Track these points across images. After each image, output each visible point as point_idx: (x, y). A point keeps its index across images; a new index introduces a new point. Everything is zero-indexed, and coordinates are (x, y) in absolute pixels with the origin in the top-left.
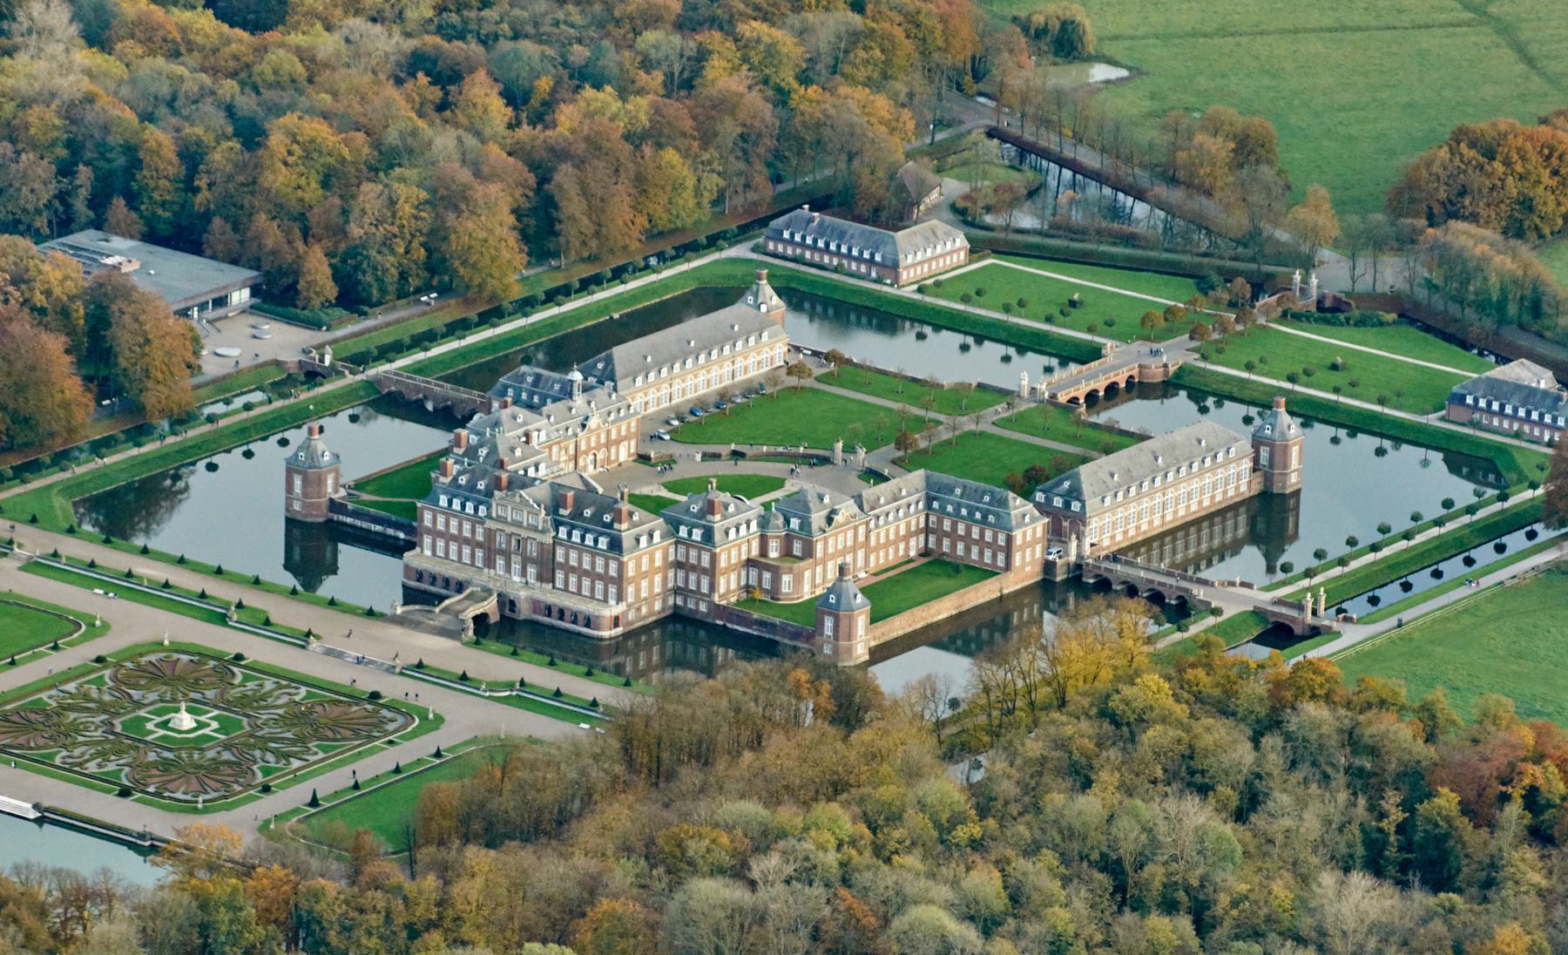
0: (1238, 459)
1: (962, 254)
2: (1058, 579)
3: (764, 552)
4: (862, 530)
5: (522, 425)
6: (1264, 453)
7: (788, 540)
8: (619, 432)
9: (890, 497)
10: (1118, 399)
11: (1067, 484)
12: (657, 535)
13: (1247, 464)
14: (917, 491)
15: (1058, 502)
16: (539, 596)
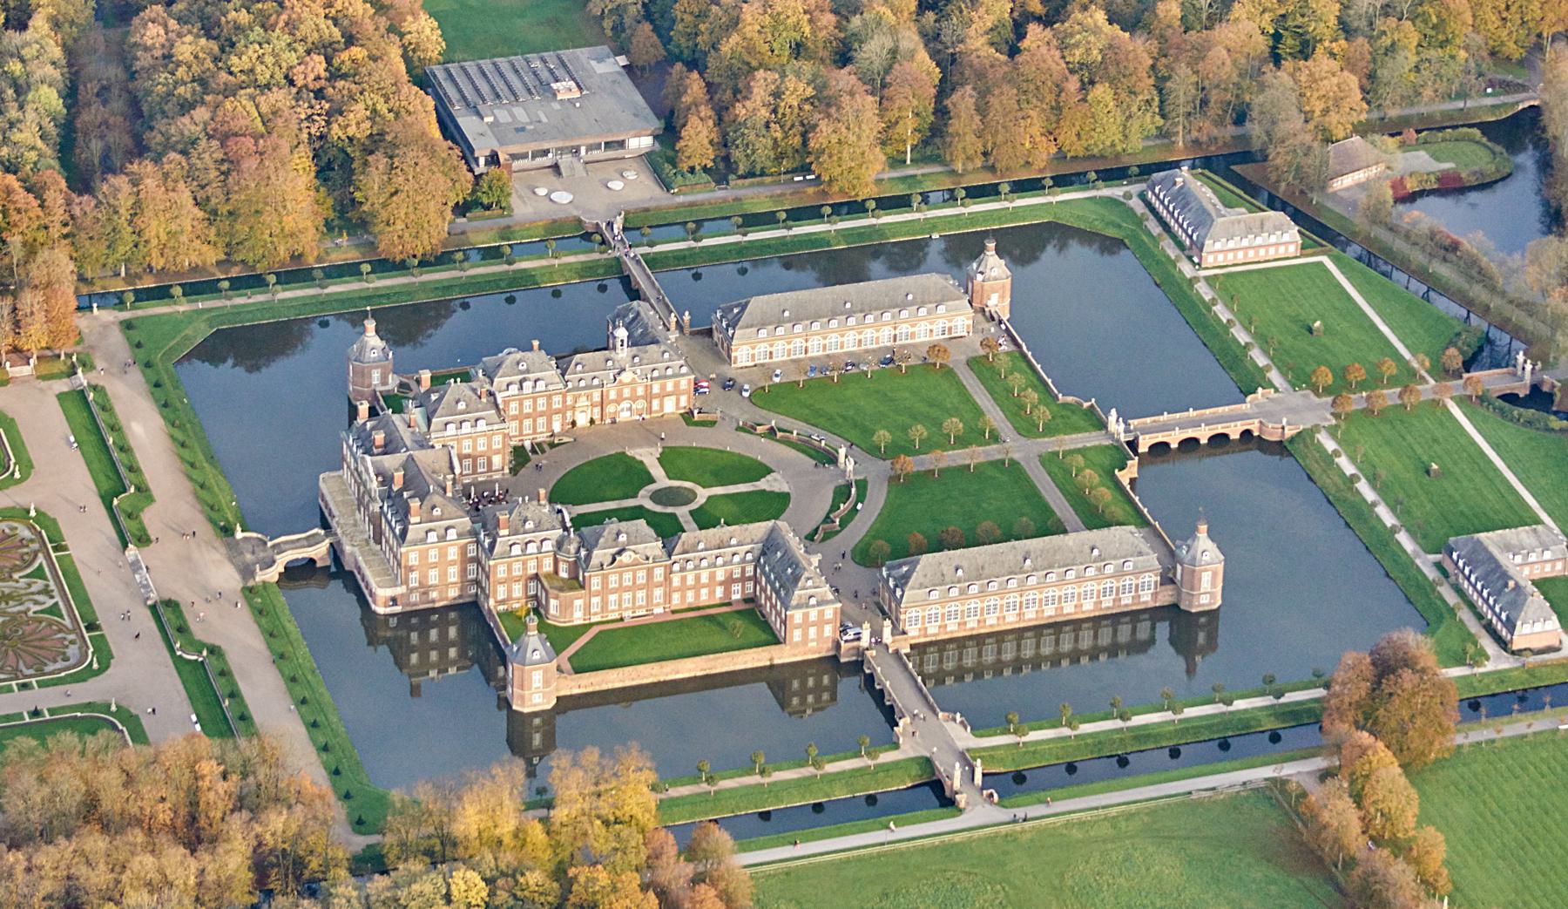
0: (1137, 573)
1: (1292, 249)
2: (843, 660)
3: (556, 572)
4: (659, 573)
5: (522, 372)
6: (1179, 568)
7: (575, 567)
8: (663, 387)
9: (716, 542)
10: (1227, 448)
11: (905, 569)
12: (452, 534)
13: (1152, 578)
14: (752, 542)
15: (891, 584)
16: (358, 554)
